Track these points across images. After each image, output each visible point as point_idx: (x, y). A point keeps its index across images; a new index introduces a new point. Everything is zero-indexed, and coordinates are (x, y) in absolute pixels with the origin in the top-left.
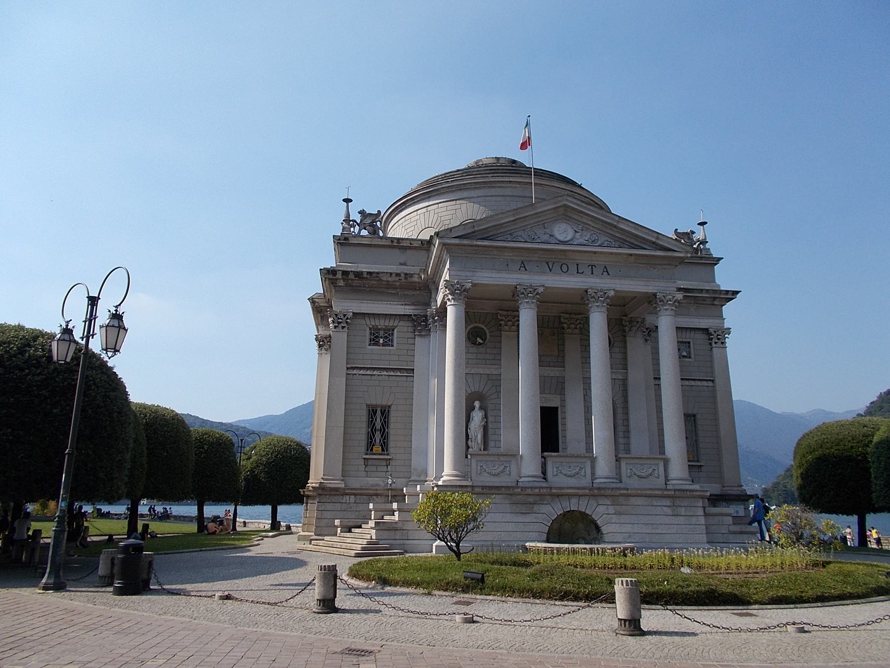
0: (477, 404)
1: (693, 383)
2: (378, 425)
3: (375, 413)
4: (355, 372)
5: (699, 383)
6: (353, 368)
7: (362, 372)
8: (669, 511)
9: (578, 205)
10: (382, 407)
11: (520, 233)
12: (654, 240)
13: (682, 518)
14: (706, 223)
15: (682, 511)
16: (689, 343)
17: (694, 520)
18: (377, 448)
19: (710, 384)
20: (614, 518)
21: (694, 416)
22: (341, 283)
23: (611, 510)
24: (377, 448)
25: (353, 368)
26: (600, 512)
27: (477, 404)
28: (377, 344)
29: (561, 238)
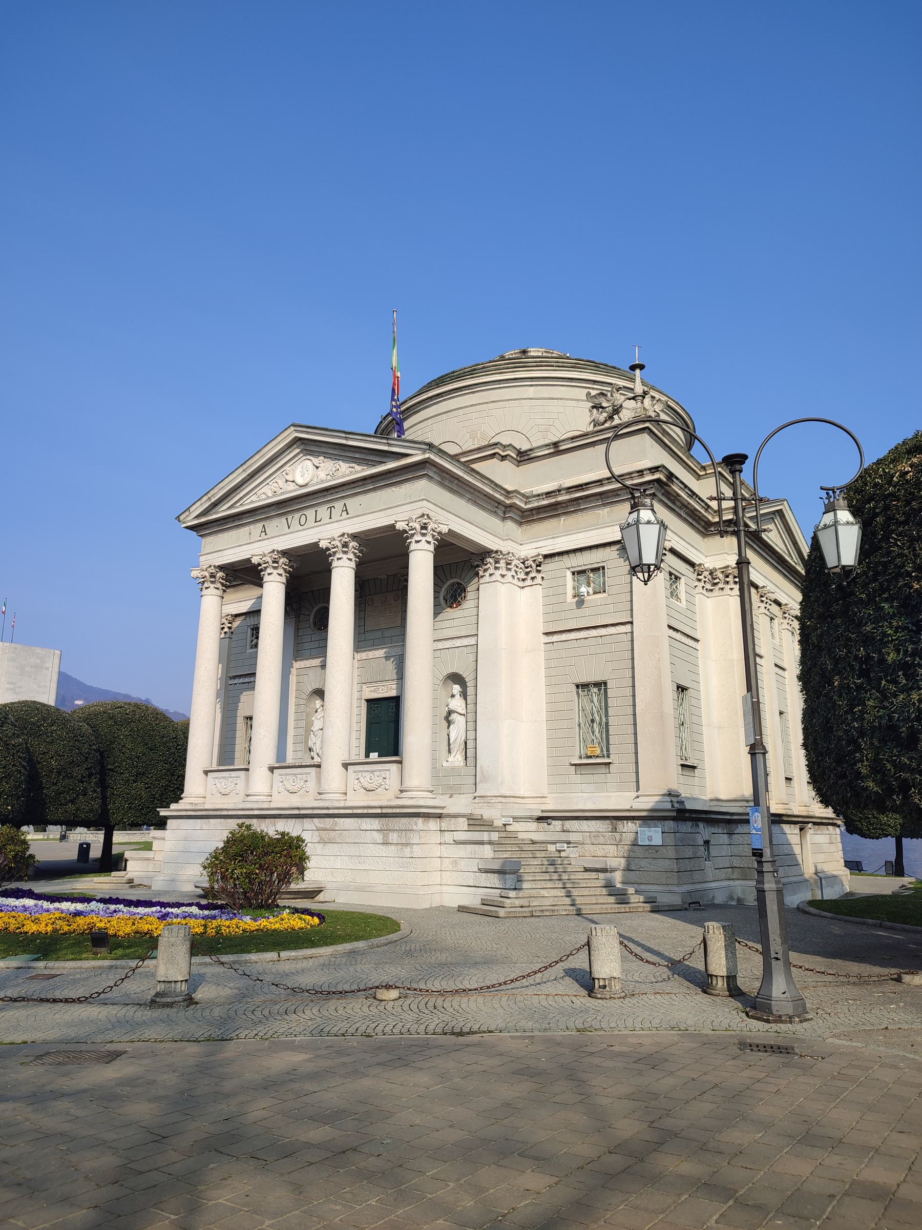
1: (603, 631)
4: (236, 681)
6: (235, 677)
7: (241, 680)
8: (378, 837)
9: (307, 433)
11: (263, 491)
12: (385, 448)
13: (393, 847)
14: (641, 367)
15: (393, 837)
16: (603, 568)
17: (407, 851)
19: (628, 628)
21: (605, 684)
25: (235, 677)
29: (300, 481)
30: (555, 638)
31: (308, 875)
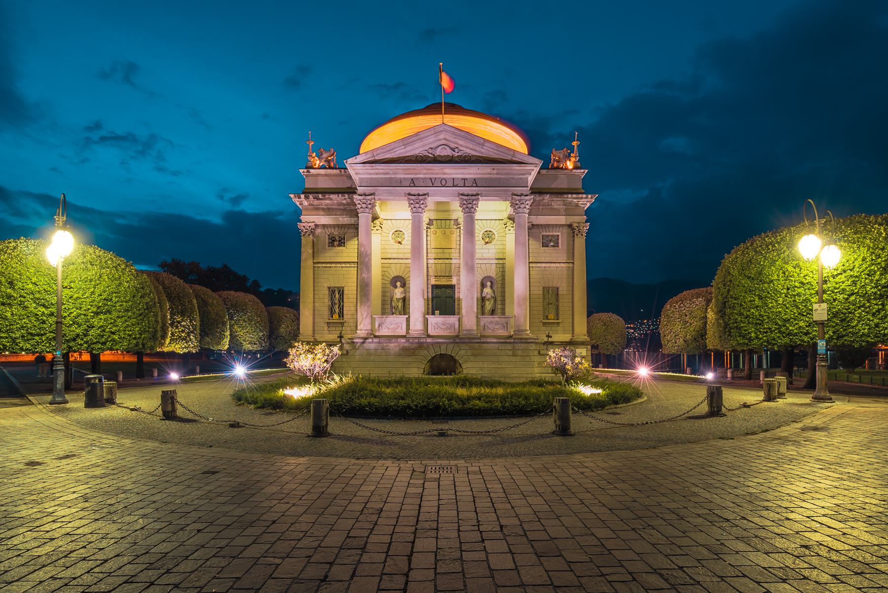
0: (398, 284)
2: (337, 302)
3: (333, 292)
5: (562, 265)
6: (318, 263)
10: (338, 288)
18: (336, 316)
19: (571, 265)
20: (472, 358)
22: (306, 203)
23: (469, 352)
24: (336, 316)
25: (318, 263)
26: (461, 353)
27: (398, 284)
28: (333, 246)
30: (534, 265)
31: (465, 372)
